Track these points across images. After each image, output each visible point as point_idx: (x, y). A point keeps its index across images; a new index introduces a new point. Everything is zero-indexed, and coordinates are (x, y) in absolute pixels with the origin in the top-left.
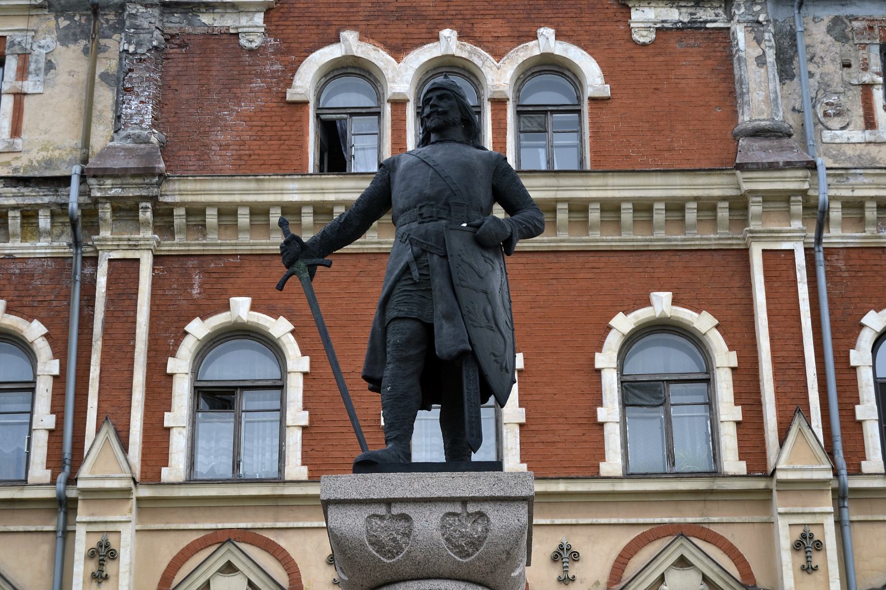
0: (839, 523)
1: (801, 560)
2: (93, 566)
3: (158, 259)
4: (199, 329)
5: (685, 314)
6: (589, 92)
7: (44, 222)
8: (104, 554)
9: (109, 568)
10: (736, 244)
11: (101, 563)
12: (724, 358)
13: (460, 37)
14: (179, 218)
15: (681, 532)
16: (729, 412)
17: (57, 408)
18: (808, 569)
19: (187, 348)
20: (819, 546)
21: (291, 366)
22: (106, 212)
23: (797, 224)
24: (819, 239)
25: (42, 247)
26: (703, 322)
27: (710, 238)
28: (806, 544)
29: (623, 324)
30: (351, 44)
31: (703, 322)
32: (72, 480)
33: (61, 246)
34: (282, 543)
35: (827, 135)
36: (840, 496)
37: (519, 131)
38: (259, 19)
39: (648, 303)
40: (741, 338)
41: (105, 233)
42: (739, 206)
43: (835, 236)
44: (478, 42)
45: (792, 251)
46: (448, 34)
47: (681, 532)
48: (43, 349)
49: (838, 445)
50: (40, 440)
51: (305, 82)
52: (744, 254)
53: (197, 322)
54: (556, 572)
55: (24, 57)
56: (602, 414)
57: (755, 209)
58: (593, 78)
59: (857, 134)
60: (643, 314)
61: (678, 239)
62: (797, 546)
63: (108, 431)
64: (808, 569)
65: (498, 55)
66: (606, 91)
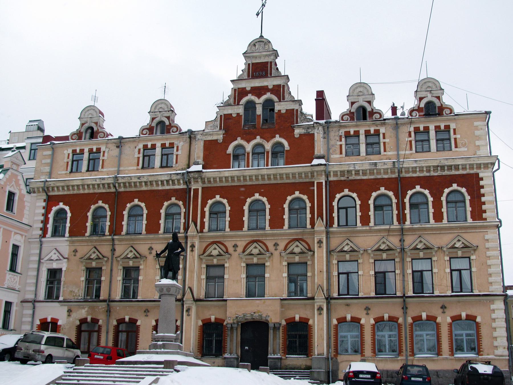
0: (327, 238)
1: (319, 245)
2: (191, 249)
3: (203, 188)
4: (210, 202)
5: (302, 196)
6: (286, 149)
7: (182, 182)
8: (193, 246)
9: (194, 249)
10: (313, 180)
11: (192, 248)
12: (309, 205)
13: (261, 138)
14: (206, 180)
15: (297, 240)
16: (309, 216)
17: (185, 218)
18: (320, 247)
19: (208, 206)
20: (322, 242)
21: (227, 209)
22: (192, 179)
23: (324, 176)
24: (328, 179)
25: (182, 186)
26: (305, 197)
27: (307, 180)
28: (320, 242)
29: (289, 198)
30: (239, 141)
31: (305, 197)
32: (187, 233)
33: (185, 187)
34: (225, 243)
35: (332, 156)
36: (327, 233)
37: (272, 157)
38: (222, 136)
39: (294, 194)
40: (312, 201)
41: (192, 183)
42: (312, 173)
43: (332, 178)
44: (264, 139)
45: (322, 182)
46: (258, 137)
47: (297, 240)
48: (182, 207)
49: (328, 222)
50: (182, 224)
51: (230, 150)
52: (314, 182)
53: (210, 200)
54: (274, 248)
55: (178, 147)
56: (284, 217)
57: (315, 174)
58: (287, 146)
59: (338, 156)
60: (293, 196)
61: (301, 181)
62: (318, 242)
63: (193, 224)
64: (320, 247)
65: (268, 141)
66: (289, 149)
